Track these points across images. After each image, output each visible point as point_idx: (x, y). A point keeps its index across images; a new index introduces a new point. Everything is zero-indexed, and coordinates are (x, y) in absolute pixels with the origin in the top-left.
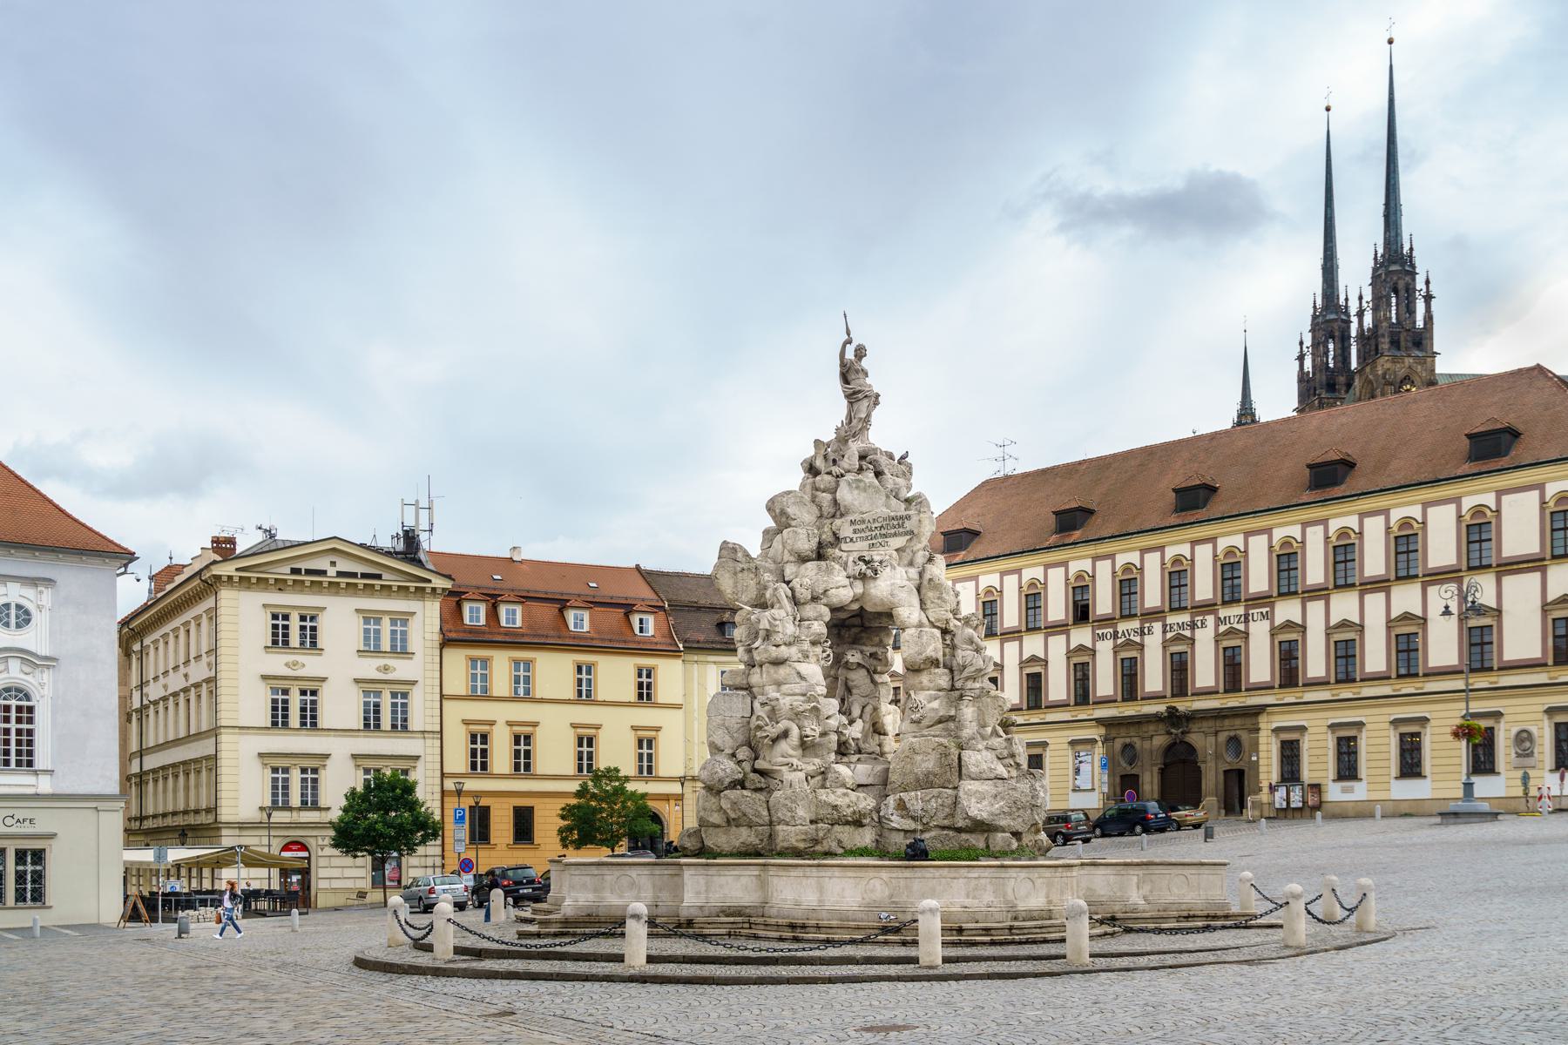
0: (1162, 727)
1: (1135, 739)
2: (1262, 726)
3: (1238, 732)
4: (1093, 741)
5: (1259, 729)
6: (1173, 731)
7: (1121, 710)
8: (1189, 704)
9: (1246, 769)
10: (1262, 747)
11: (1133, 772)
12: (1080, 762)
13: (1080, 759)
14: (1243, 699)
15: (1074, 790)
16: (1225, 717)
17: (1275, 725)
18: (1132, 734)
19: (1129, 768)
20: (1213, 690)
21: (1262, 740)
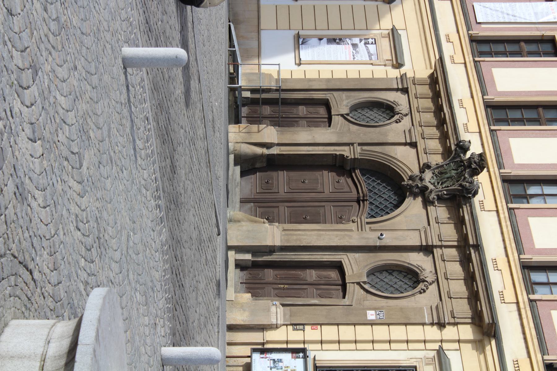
0: (437, 160)
1: (406, 121)
2: (450, 332)
3: (433, 288)
4: (399, 65)
5: (441, 325)
6: (428, 175)
7: (468, 103)
8: (490, 204)
9: (346, 301)
10: (398, 332)
11: (336, 119)
12: (355, 46)
13: (361, 45)
14: (510, 296)
15: (298, 36)
16: (465, 261)
17: (453, 357)
18: (416, 116)
19: (345, 110)
20: (526, 246)
21: (415, 332)
